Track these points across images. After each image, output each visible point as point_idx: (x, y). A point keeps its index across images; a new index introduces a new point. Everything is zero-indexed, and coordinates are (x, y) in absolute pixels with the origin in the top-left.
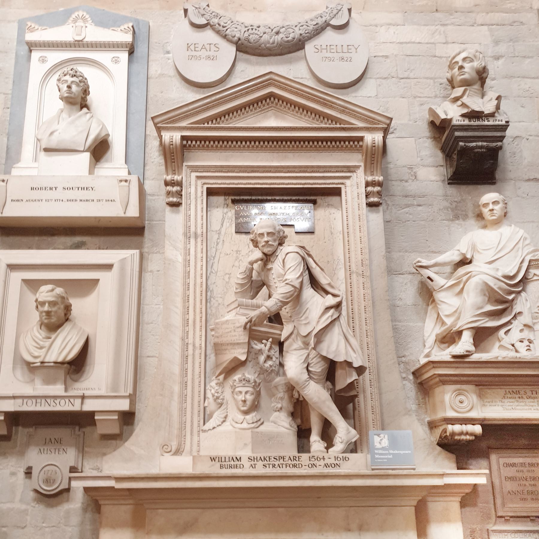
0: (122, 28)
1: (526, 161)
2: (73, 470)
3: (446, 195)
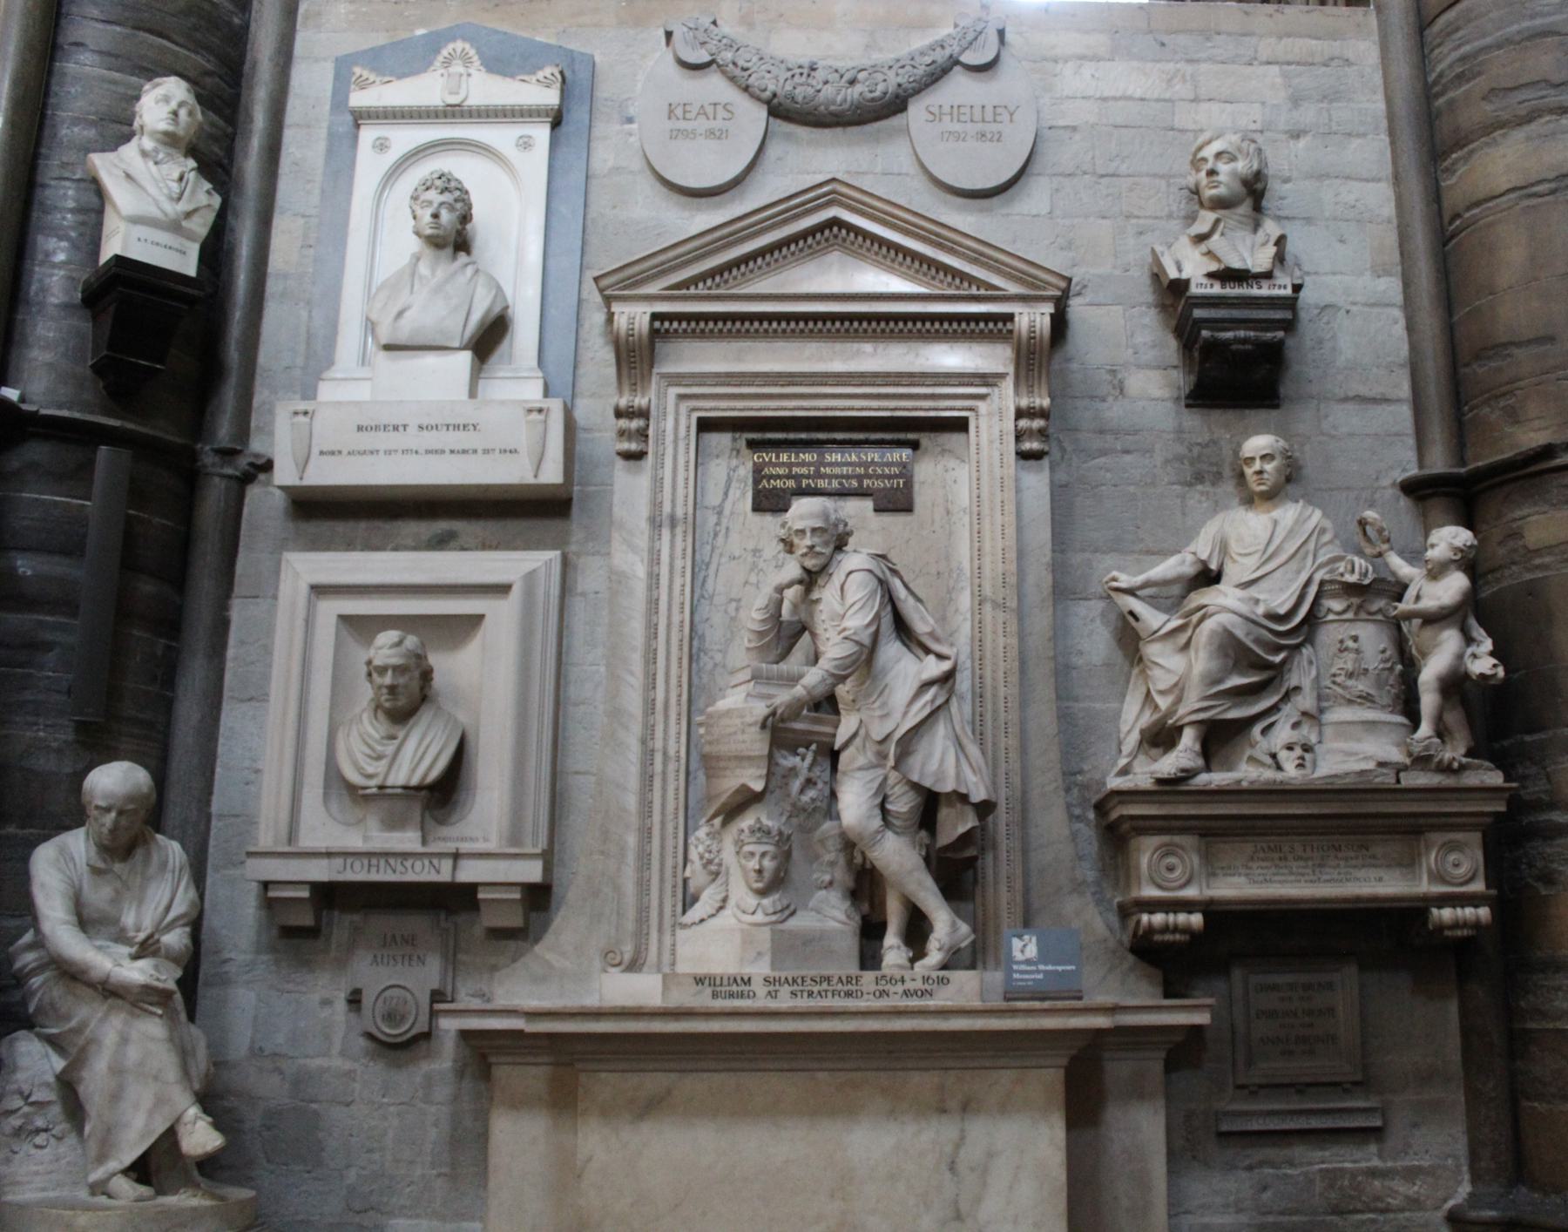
0: (540, 75)
1: (1343, 358)
2: (438, 998)
3: (1179, 431)
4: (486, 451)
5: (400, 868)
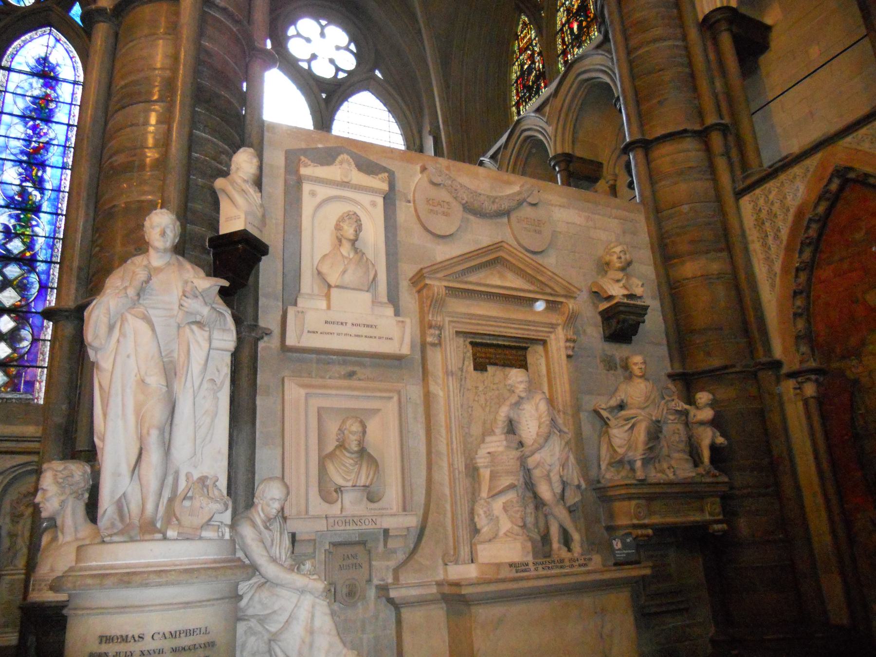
0: (380, 176)
4: (380, 338)
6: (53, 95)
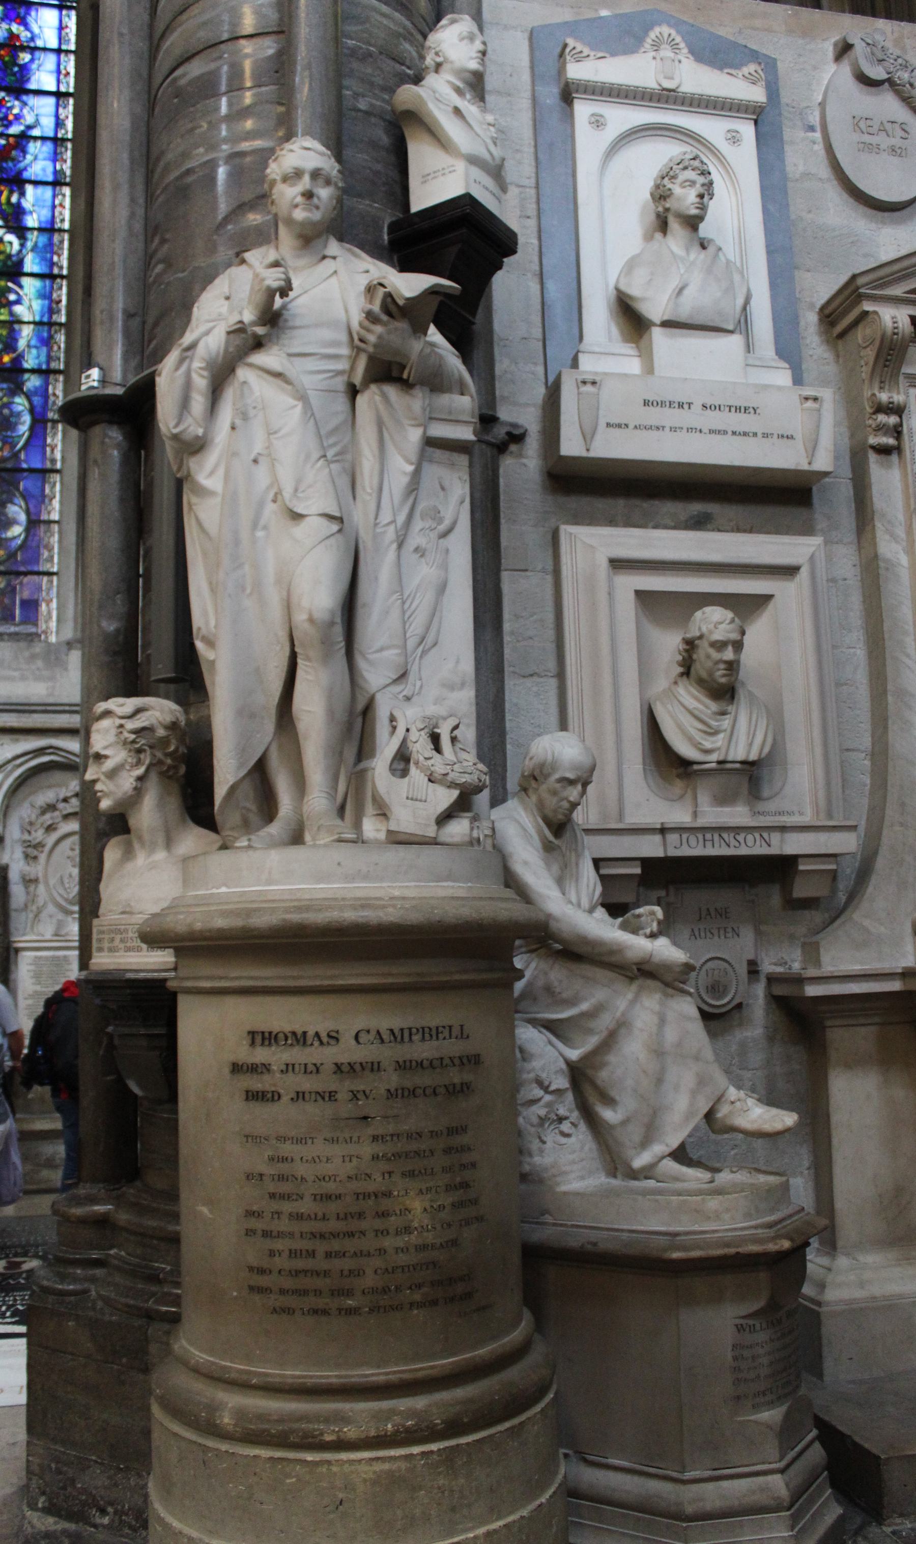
4: (765, 435)
5: (733, 842)
6: (24, 35)
